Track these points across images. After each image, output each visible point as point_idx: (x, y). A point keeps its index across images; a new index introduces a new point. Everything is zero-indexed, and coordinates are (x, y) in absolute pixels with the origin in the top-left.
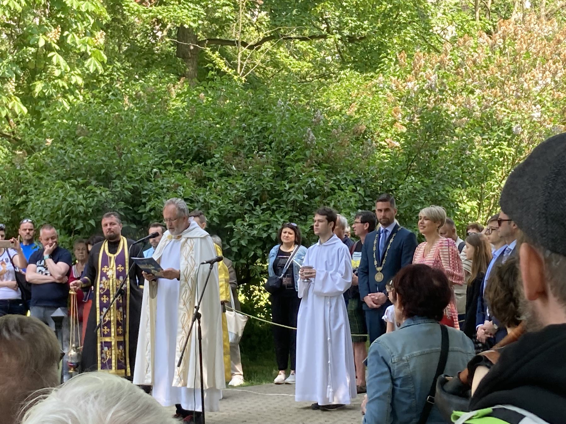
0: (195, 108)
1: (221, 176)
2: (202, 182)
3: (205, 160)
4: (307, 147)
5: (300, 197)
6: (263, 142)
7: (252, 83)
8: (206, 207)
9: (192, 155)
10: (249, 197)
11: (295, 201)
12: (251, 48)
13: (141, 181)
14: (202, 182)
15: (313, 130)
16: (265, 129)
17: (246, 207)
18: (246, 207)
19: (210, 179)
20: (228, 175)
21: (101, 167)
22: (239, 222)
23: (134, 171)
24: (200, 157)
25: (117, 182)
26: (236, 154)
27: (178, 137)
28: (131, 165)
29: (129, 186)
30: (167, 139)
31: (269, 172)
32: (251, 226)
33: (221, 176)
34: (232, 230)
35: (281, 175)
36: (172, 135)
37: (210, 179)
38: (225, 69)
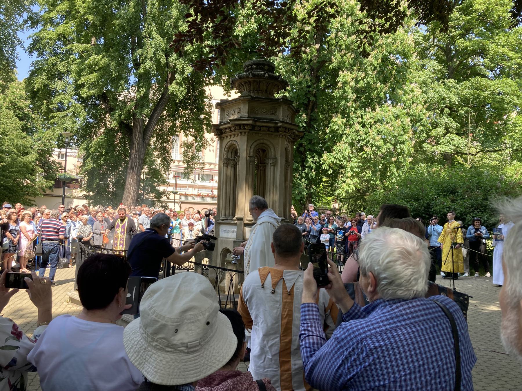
0: (451, 177)
1: (461, 199)
2: (453, 201)
3: (455, 193)
6: (478, 186)
8: (455, 210)
9: (449, 191)
10: (472, 207)
13: (430, 200)
14: (453, 201)
15: (500, 182)
16: (479, 182)
17: (471, 210)
18: (471, 210)
19: (457, 200)
20: (464, 199)
21: (416, 195)
22: (468, 215)
23: (428, 197)
25: (422, 200)
26: (467, 191)
27: (444, 185)
28: (427, 195)
29: (425, 202)
30: (440, 186)
31: (481, 197)
32: (473, 217)
33: (461, 199)
34: (465, 218)
36: (442, 184)
37: (457, 200)
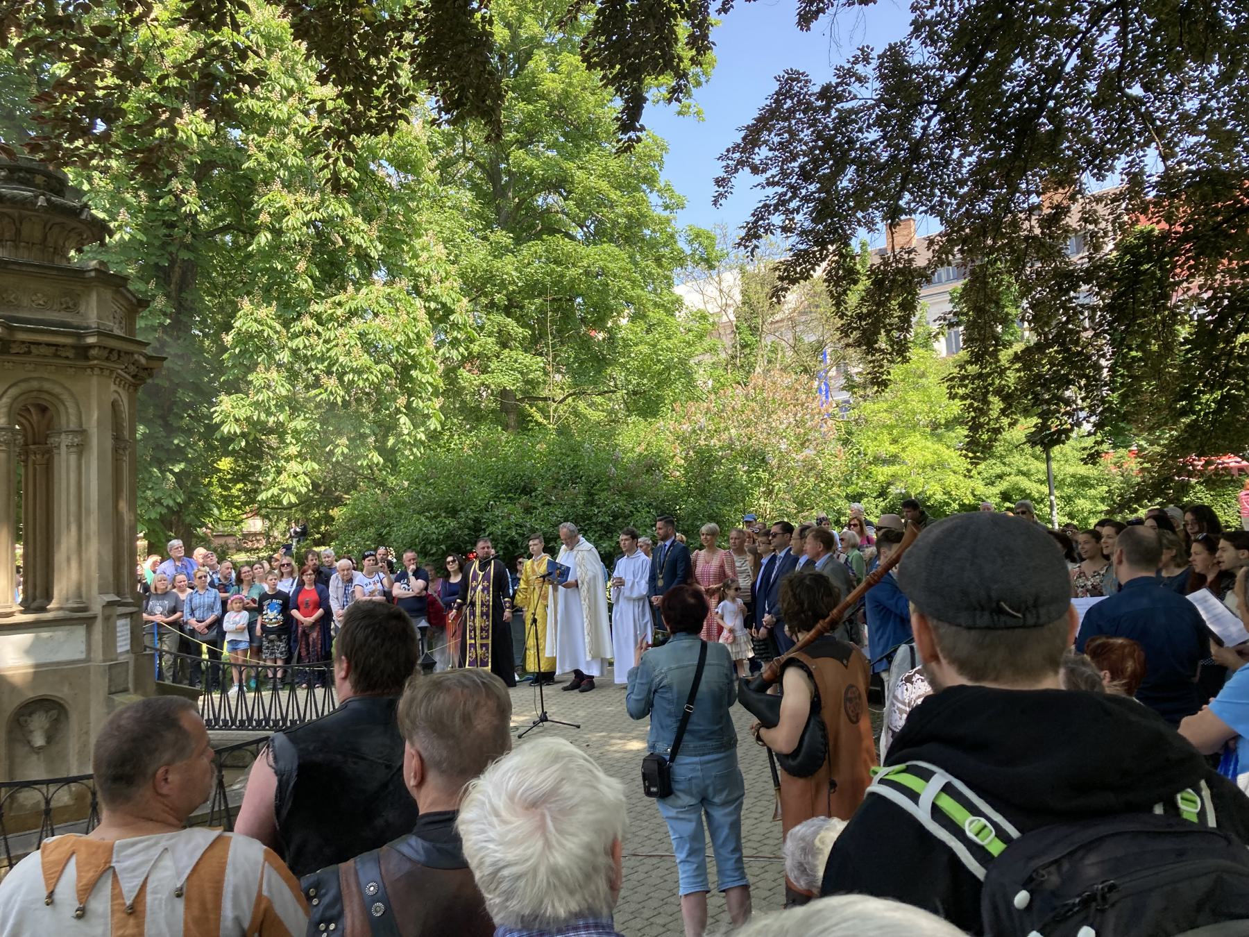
3: (531, 491)
4: (610, 479)
5: (607, 519)
7: (563, 431)
11: (601, 523)
12: (561, 402)
13: (481, 511)
14: (528, 510)
16: (576, 466)
19: (535, 508)
20: (549, 504)
24: (527, 490)
25: (462, 514)
26: (555, 487)
27: (509, 475)
31: (581, 501)
35: (590, 502)
37: (535, 508)
38: (540, 420)
